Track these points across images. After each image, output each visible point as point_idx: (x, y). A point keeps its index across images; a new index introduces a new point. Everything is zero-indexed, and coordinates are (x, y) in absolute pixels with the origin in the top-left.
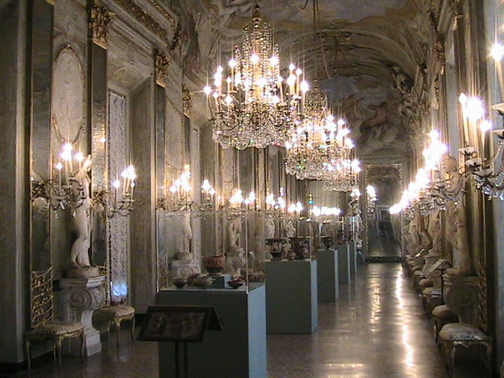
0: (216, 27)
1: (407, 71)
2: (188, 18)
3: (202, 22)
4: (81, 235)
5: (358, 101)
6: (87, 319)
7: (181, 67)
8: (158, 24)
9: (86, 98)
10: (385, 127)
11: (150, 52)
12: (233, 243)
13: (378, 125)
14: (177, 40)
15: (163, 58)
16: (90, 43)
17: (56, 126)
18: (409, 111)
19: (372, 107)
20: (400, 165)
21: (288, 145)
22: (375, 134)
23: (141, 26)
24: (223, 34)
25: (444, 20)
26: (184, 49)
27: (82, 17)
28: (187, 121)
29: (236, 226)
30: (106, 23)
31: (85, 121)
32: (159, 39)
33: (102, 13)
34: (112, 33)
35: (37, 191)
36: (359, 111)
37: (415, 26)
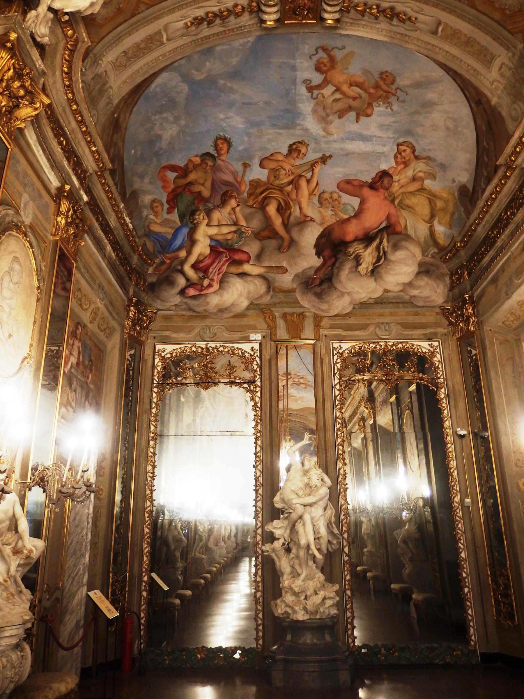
5: (313, 165)
10: (385, 241)
13: (367, 239)
19: (349, 186)
20: (436, 344)
22: (358, 260)
36: (315, 199)
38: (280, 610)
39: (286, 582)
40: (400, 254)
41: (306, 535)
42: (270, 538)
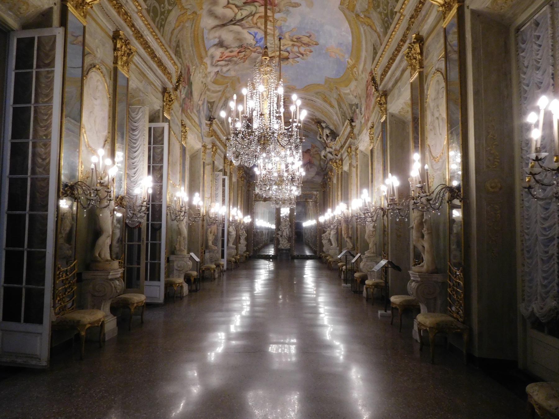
0: (204, 80)
1: (332, 127)
2: (187, 69)
3: (196, 74)
4: (104, 233)
6: (107, 307)
7: (181, 106)
8: (166, 68)
9: (111, 117)
11: (160, 89)
12: (210, 243)
14: (179, 85)
15: (170, 96)
16: (116, 69)
17: (85, 135)
18: (329, 155)
21: (257, 171)
23: (154, 66)
24: (209, 87)
25: (390, 78)
26: (182, 93)
27: (109, 44)
28: (183, 149)
29: (213, 232)
30: (129, 55)
31: (110, 135)
32: (166, 80)
33: (126, 45)
34: (132, 66)
35: (66, 191)
37: (348, 91)
38: (279, 247)
39: (281, 242)
40: (312, 169)
41: (285, 234)
42: (278, 234)
